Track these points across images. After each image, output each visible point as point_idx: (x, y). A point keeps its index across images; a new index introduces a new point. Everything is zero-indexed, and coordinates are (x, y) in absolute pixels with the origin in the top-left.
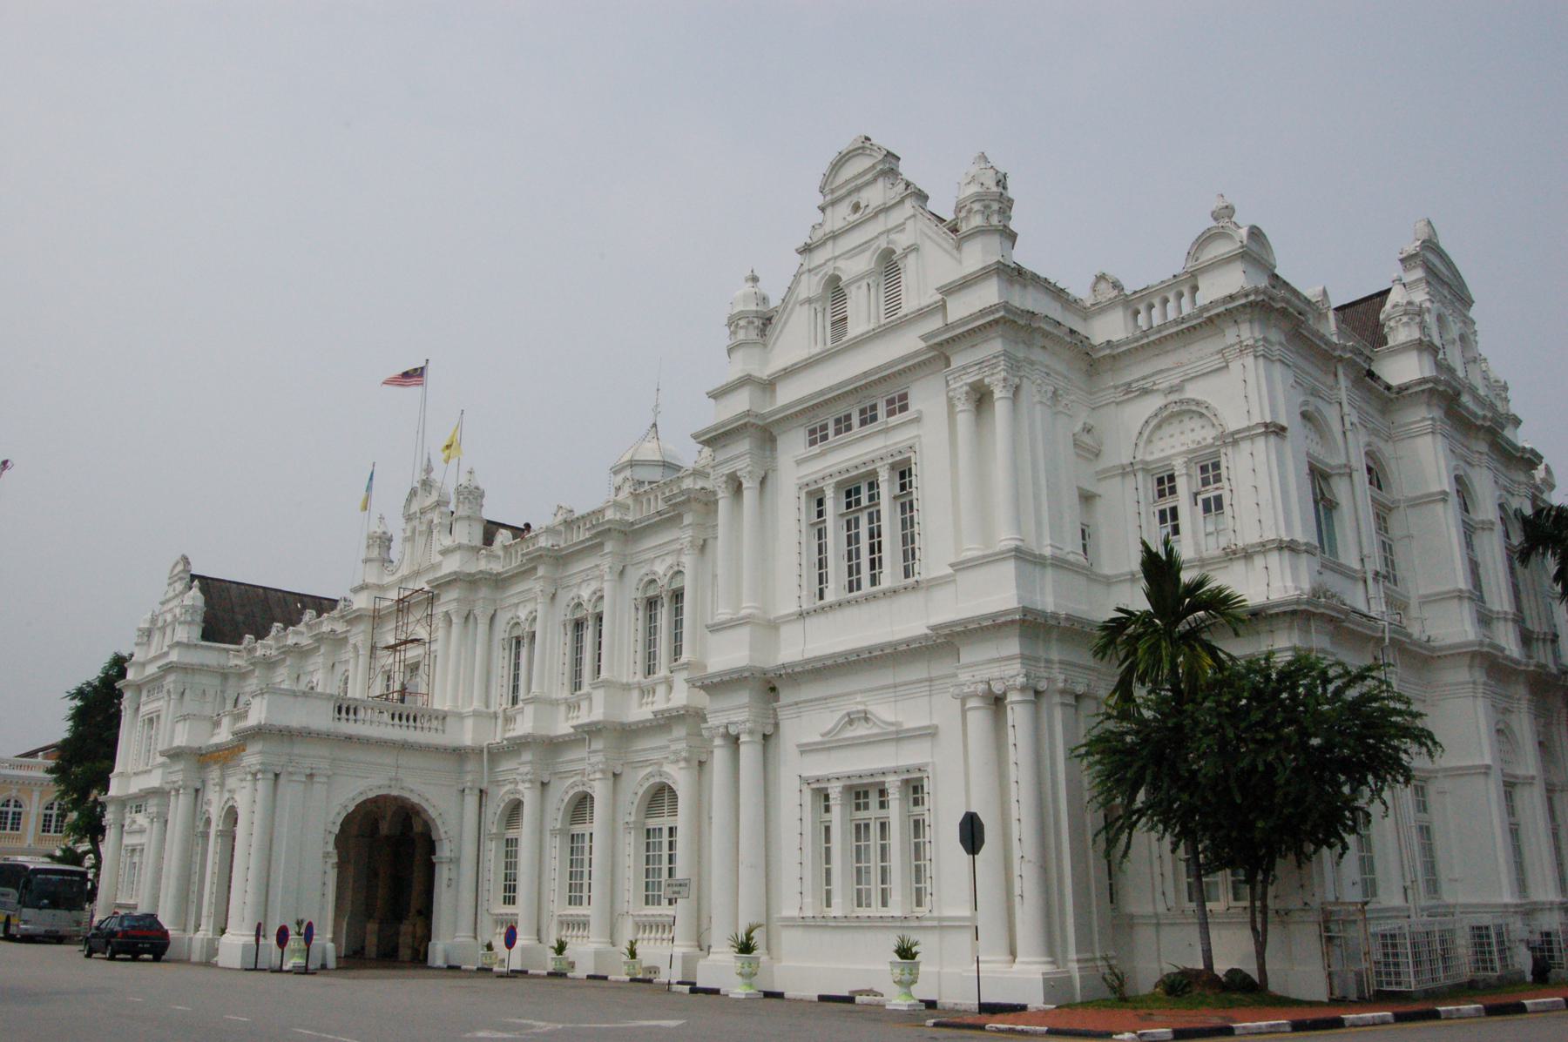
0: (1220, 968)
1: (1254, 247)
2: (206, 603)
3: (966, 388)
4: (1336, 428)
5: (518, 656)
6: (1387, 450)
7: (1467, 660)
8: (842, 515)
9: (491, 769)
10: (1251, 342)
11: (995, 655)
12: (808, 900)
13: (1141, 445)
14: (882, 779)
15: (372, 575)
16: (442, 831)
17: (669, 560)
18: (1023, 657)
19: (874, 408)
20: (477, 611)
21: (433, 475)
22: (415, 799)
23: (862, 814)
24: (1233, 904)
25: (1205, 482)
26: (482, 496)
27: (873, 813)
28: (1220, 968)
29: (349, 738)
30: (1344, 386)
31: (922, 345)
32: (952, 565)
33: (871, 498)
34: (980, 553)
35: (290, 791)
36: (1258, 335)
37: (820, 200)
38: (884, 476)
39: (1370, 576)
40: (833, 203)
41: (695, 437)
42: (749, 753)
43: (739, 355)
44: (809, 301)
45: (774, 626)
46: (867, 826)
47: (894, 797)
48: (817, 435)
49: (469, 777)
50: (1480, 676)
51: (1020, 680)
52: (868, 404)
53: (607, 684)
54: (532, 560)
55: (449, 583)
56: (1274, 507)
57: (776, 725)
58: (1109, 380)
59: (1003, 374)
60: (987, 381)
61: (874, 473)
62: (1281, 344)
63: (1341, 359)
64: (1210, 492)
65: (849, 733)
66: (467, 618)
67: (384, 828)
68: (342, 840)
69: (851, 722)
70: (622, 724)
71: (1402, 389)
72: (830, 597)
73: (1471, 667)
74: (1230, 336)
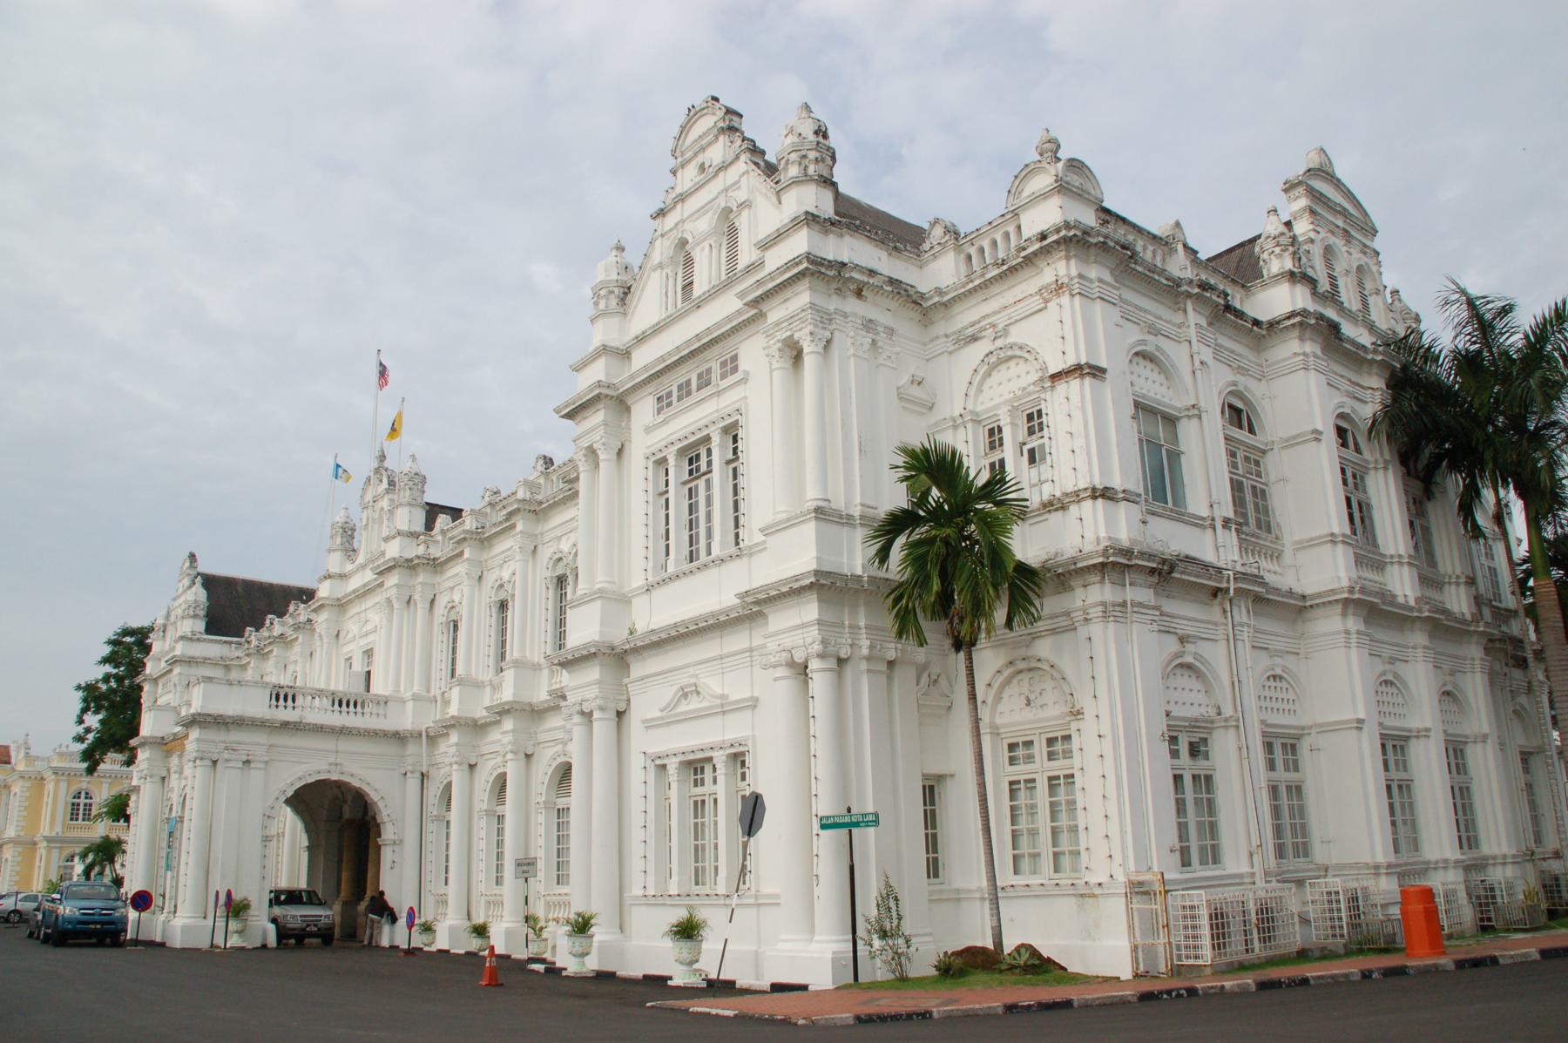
0: (1009, 945)
1: (1075, 180)
2: (209, 598)
4: (1184, 367)
5: (455, 640)
6: (1256, 390)
7: (1338, 608)
8: (684, 483)
9: (430, 756)
11: (799, 622)
12: (651, 879)
13: (972, 393)
15: (335, 563)
16: (384, 814)
18: (820, 622)
19: (709, 371)
20: (417, 597)
22: (356, 783)
23: (699, 790)
24: (1053, 875)
25: (1031, 432)
26: (424, 480)
27: (708, 787)
28: (1009, 945)
29: (285, 725)
30: (1194, 318)
31: (738, 304)
32: (761, 530)
34: (784, 516)
36: (1074, 272)
37: (672, 163)
38: (716, 440)
39: (1219, 524)
40: (683, 166)
41: (557, 411)
42: (602, 728)
43: (600, 323)
44: (661, 266)
45: (624, 600)
46: (703, 802)
47: (721, 770)
49: (410, 760)
50: (1354, 624)
51: (817, 647)
52: (703, 368)
53: (518, 664)
54: (459, 542)
55: (390, 569)
56: (1088, 454)
58: (941, 328)
59: (811, 328)
60: (796, 336)
61: (707, 439)
62: (1101, 281)
63: (1189, 295)
64: (1034, 443)
65: (683, 707)
67: (347, 814)
69: (685, 695)
70: (530, 704)
71: (1272, 325)
72: (671, 569)
73: (1344, 614)
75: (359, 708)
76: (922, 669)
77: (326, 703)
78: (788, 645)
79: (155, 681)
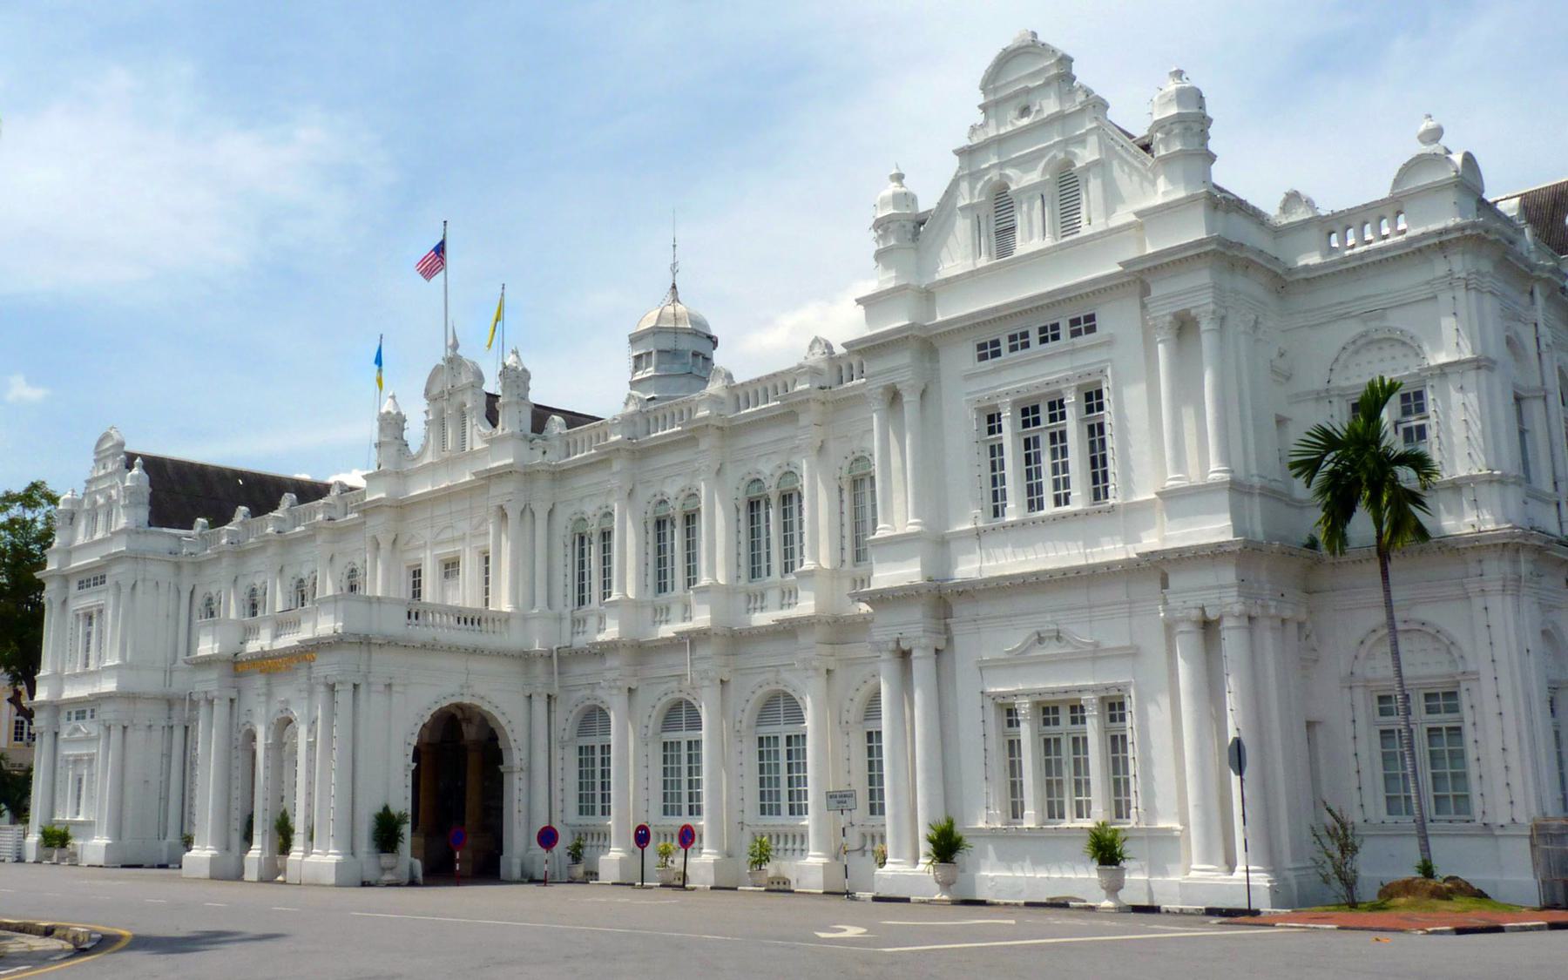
3: (1168, 318)
8: (1019, 434)
10: (1463, 275)
14: (1077, 695)
17: (777, 460)
20: (536, 506)
21: (459, 352)
22: (486, 707)
23: (1052, 728)
33: (1053, 418)
35: (373, 704)
38: (1070, 399)
46: (1057, 741)
48: (988, 351)
57: (949, 641)
60: (1193, 312)
64: (1414, 422)
65: (1038, 652)
66: (522, 512)
68: (417, 755)
69: (1041, 640)
74: (1440, 268)
75: (483, 624)
76: (1301, 625)
77: (453, 621)
78: (1200, 603)
79: (93, 579)
